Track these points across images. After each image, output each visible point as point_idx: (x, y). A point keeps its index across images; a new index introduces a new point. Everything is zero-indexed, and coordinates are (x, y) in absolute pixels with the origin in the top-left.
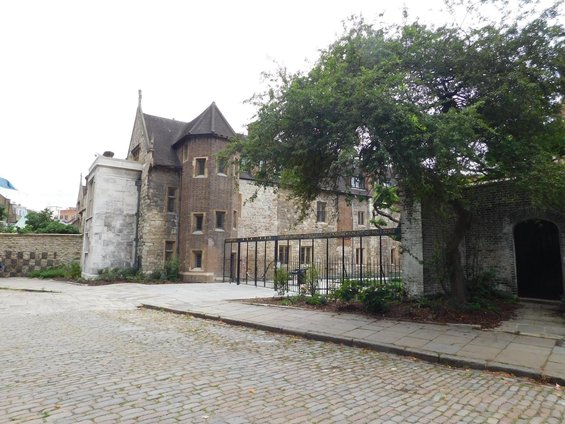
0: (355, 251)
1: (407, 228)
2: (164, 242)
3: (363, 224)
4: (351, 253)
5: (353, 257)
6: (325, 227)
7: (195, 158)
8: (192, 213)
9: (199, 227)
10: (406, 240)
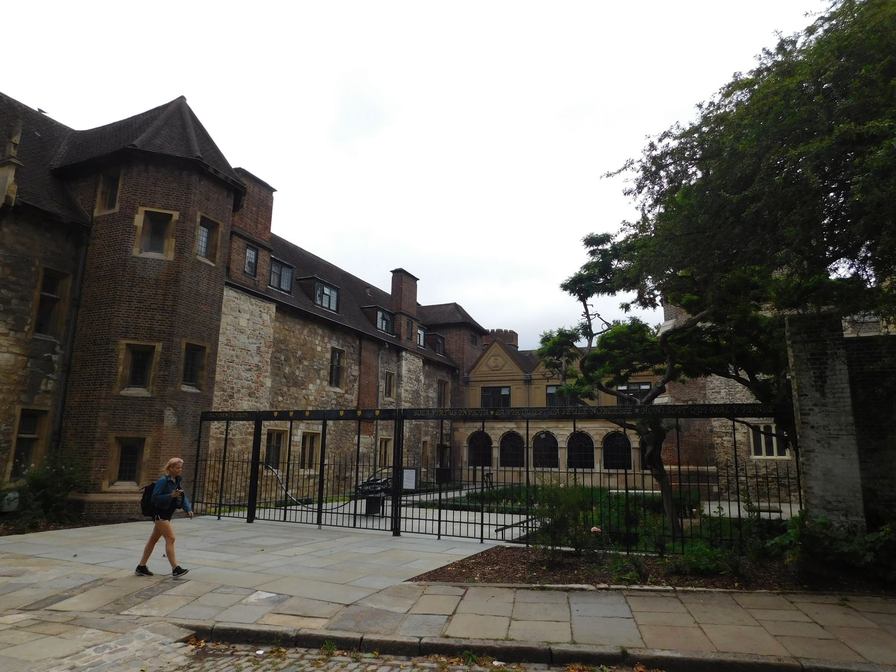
0: (379, 444)
1: (815, 405)
2: (18, 410)
3: (390, 396)
4: (374, 447)
5: (376, 455)
6: (340, 397)
7: (142, 210)
8: (124, 342)
9: (138, 377)
10: (813, 427)
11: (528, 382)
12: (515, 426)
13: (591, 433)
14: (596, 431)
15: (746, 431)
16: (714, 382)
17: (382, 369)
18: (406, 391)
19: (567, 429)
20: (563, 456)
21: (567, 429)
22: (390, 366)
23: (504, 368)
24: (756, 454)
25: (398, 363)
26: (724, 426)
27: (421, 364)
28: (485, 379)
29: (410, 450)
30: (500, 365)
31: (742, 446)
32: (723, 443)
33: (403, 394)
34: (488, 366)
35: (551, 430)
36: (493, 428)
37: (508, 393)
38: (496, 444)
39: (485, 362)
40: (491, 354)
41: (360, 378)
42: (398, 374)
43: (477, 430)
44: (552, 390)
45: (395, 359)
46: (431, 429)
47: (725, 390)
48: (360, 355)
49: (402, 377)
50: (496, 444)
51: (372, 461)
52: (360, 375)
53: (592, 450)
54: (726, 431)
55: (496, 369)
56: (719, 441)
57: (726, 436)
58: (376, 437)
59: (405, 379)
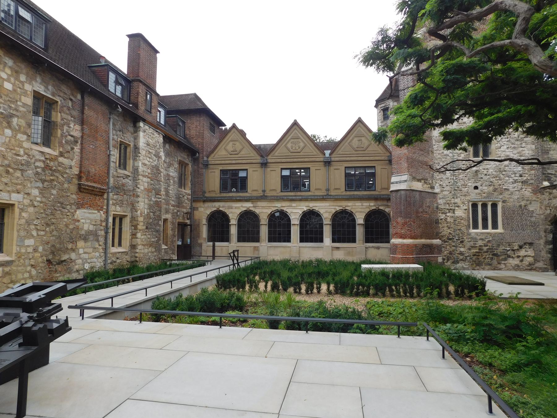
0: (111, 220)
3: (125, 168)
4: (104, 224)
5: (107, 233)
6: (51, 160)
11: (264, 165)
12: (252, 205)
13: (322, 211)
14: (327, 210)
15: (466, 208)
17: (114, 137)
18: (144, 164)
19: (300, 207)
20: (295, 232)
21: (300, 207)
22: (125, 135)
23: (242, 153)
24: (474, 228)
25: (136, 134)
26: (448, 204)
27: (161, 139)
28: (223, 162)
29: (149, 227)
30: (238, 150)
31: (462, 221)
32: (446, 219)
33: (140, 167)
34: (226, 150)
35: (285, 209)
36: (232, 208)
38: (234, 221)
39: (224, 146)
40: (230, 139)
41: (82, 141)
43: (215, 209)
44: (286, 173)
45: (131, 129)
46: (172, 208)
49: (139, 149)
50: (234, 221)
51: (102, 240)
52: (82, 137)
56: (443, 216)
57: (449, 212)
58: (107, 212)
59: (143, 152)
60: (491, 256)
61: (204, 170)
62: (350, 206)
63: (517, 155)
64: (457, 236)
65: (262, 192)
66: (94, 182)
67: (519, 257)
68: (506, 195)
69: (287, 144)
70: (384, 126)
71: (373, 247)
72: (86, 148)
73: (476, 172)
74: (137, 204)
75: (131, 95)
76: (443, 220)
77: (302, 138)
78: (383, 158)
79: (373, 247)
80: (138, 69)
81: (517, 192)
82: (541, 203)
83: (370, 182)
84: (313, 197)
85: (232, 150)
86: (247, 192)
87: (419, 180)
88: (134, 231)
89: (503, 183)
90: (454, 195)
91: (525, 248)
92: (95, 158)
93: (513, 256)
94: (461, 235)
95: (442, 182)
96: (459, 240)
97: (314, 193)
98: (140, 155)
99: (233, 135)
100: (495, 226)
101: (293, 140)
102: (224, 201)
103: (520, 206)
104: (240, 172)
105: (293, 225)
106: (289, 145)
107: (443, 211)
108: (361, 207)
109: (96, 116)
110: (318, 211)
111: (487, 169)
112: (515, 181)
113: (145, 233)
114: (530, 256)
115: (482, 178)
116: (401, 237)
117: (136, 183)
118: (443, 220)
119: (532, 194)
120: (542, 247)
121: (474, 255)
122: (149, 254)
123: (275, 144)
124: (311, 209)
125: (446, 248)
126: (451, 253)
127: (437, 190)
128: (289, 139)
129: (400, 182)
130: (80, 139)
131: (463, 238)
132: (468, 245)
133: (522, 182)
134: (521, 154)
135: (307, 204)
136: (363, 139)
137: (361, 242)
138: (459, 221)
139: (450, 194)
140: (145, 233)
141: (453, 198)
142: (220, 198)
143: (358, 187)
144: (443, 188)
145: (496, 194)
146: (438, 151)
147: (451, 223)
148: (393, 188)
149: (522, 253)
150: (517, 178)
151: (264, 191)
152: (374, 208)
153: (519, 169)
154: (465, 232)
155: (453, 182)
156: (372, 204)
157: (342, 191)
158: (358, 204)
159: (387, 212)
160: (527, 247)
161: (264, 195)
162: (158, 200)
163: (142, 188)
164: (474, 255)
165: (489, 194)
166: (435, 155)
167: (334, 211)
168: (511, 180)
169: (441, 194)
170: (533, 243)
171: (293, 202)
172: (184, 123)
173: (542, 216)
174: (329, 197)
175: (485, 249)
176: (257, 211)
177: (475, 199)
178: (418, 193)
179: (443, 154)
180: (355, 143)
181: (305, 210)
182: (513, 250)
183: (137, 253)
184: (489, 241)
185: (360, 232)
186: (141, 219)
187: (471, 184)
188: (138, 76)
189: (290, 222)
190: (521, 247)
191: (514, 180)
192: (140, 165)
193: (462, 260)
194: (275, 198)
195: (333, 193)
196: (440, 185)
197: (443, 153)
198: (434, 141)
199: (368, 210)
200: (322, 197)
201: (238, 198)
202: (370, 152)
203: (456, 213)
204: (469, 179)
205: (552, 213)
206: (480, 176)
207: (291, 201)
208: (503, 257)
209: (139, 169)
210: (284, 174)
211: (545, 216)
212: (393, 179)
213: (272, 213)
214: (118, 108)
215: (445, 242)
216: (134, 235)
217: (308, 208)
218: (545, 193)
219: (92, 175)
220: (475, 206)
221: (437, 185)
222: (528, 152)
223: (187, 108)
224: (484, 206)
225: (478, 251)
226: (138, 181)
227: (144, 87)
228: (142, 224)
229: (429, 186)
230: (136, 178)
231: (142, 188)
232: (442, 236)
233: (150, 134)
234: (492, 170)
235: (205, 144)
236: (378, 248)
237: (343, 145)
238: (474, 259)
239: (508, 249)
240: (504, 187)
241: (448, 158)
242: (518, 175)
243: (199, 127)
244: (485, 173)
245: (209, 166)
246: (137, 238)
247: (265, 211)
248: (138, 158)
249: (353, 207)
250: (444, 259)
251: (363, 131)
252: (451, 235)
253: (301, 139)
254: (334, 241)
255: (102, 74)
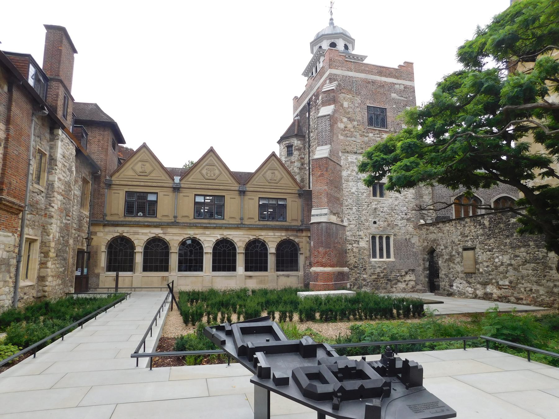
3: (38, 184)
4: (17, 250)
5: (19, 262)
12: (162, 232)
13: (236, 240)
14: (240, 238)
15: (368, 240)
16: (349, 200)
18: (59, 179)
19: (213, 235)
21: (213, 235)
23: (152, 175)
24: (373, 258)
25: (52, 143)
28: (130, 183)
29: (59, 254)
30: (148, 171)
31: (365, 251)
32: (353, 249)
33: (56, 182)
34: (134, 171)
35: (198, 237)
36: (137, 233)
37: (155, 199)
38: (139, 249)
39: (131, 166)
40: (139, 159)
42: (50, 156)
43: (118, 234)
44: (200, 199)
45: (48, 136)
46: (74, 231)
47: (356, 207)
48: (9, 109)
50: (139, 249)
51: (13, 270)
52: (7, 139)
53: (234, 255)
54: (355, 240)
55: (143, 174)
56: (350, 247)
58: (21, 235)
59: (60, 165)
60: (386, 281)
61: (106, 190)
62: (263, 235)
63: (403, 197)
64: (361, 264)
65: (173, 218)
66: (15, 197)
67: (405, 281)
68: (396, 229)
69: (265, 173)
70: (288, 161)
71: (283, 275)
72: (10, 154)
73: (375, 209)
74: (49, 226)
75: (48, 95)
76: (350, 250)
77: (217, 165)
78: (293, 191)
79: (283, 275)
80: (59, 68)
81: (404, 228)
82: (419, 237)
83: (265, 213)
84: (228, 226)
85: (141, 170)
86: (156, 217)
87: (334, 214)
88: (43, 259)
89: (394, 220)
90: (359, 228)
91: (409, 273)
92: (17, 167)
93: (402, 280)
94: (364, 263)
95: (349, 217)
96: (362, 267)
97: (228, 221)
98: (56, 167)
99: (143, 155)
100: (388, 256)
101: (208, 167)
102: (129, 226)
103: (406, 239)
104: (149, 195)
105: (206, 254)
106: (204, 172)
107: (350, 242)
108: (273, 237)
109: (21, 115)
110: (232, 240)
111: (383, 207)
112: (402, 219)
113: (54, 262)
114: (412, 280)
115: (379, 215)
116: (322, 266)
117: (50, 201)
118: (350, 250)
119: (413, 229)
120: (421, 272)
121: (374, 281)
122: (57, 287)
123: (253, 173)
124: (225, 237)
125: (353, 275)
126: (356, 280)
127: (345, 224)
128: (204, 164)
129: (321, 215)
130: (4, 141)
131: (365, 266)
132: (369, 272)
133: (407, 220)
134: (406, 197)
135: (221, 232)
136: (276, 172)
137: (273, 270)
138: (363, 251)
139: (356, 228)
140: (54, 262)
141: (358, 231)
142: (125, 223)
143: (272, 217)
144: (350, 221)
145: (389, 228)
146: (346, 189)
147: (356, 253)
148: (313, 220)
149: (407, 278)
150: (403, 216)
151: (175, 217)
152: (285, 238)
153: (405, 209)
154: (367, 260)
155: (358, 217)
156: (283, 234)
157: (255, 221)
158: (271, 233)
159: (296, 242)
160: (411, 273)
161: (175, 221)
162: (67, 222)
163: (56, 207)
164: (374, 281)
165: (385, 229)
166: (344, 192)
167: (247, 240)
168: (400, 218)
169: (349, 227)
170: (414, 270)
171: (207, 229)
172: (87, 134)
173: (421, 248)
174: (243, 226)
175: (382, 275)
176: (167, 238)
177: (374, 232)
178: (334, 226)
179: (350, 192)
180: (269, 175)
181: (219, 238)
182: (401, 276)
183: (46, 286)
184: (385, 269)
185: (271, 261)
186: (53, 245)
187: (372, 220)
188: (58, 75)
189: (203, 250)
190: (406, 273)
191: (401, 217)
192: (56, 179)
193: (364, 285)
194: (188, 225)
195: (246, 222)
196: (348, 219)
197: (350, 191)
198: (343, 180)
199: (279, 240)
200: (236, 226)
201: (146, 224)
202: (282, 185)
203: (360, 244)
204: (370, 215)
205: (429, 245)
206: (378, 213)
207: (205, 228)
208: (394, 282)
209: (54, 185)
210: (198, 201)
211: (423, 247)
212: (314, 212)
213: (184, 240)
214: (45, 110)
215: (352, 269)
216: (43, 264)
217: (222, 236)
218: (423, 229)
219: (13, 188)
220: (374, 238)
221: (346, 219)
222: (410, 195)
223: (88, 119)
224: (381, 238)
225: (376, 277)
226: (52, 199)
227: (63, 89)
228: (53, 250)
229: (340, 219)
230: (50, 195)
231: (56, 207)
232: (350, 265)
233: (66, 144)
234: (386, 209)
235: (108, 161)
236: (288, 276)
237: (258, 176)
238: (374, 284)
239: (398, 275)
240: (395, 223)
241: (354, 195)
242: (404, 214)
243: (102, 142)
244: (381, 210)
245: (112, 186)
246: (47, 268)
247: (176, 238)
248: (53, 171)
249: (266, 236)
250: (351, 285)
251: (276, 164)
252: (356, 264)
253: (217, 167)
254: (247, 269)
255: (21, 64)
